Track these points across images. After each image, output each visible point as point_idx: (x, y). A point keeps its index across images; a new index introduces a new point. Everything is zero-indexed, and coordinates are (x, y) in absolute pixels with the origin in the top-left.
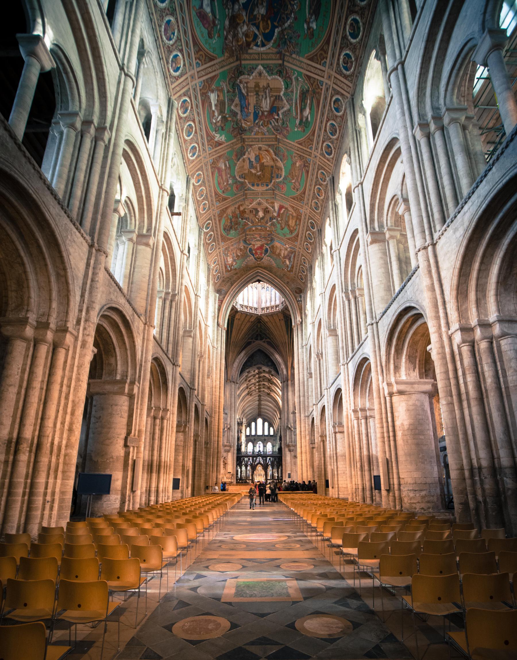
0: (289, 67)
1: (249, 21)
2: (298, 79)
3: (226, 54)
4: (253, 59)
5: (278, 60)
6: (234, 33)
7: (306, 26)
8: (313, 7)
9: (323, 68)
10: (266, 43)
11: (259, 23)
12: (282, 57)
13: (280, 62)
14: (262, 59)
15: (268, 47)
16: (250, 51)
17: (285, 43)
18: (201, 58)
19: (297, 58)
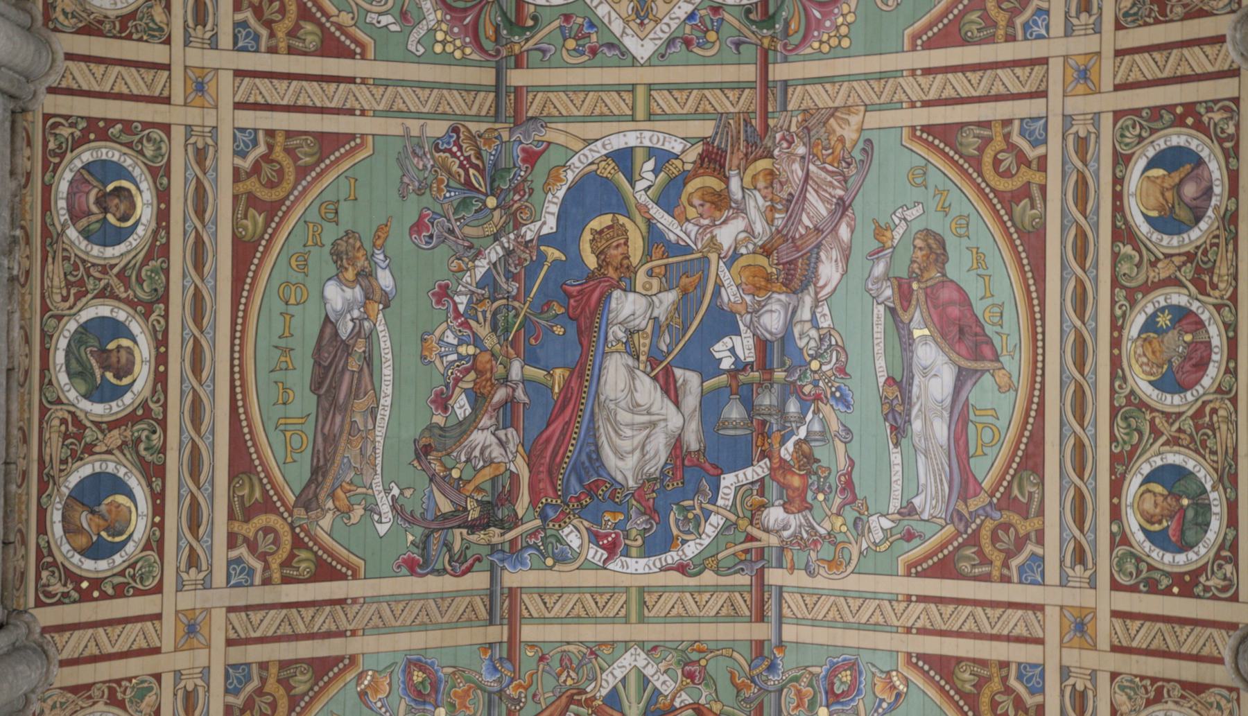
0: (464, 62)
1: (705, 259)
2: (403, 16)
3: (850, 134)
4: (686, 87)
5: (537, 89)
6: (794, 219)
7: (385, 279)
8: (354, 365)
9: (248, 119)
10: (608, 169)
11: (648, 255)
12: (509, 103)
13: (517, 78)
14: (632, 88)
15: (599, 150)
16: (706, 128)
17: (495, 174)
18: (1008, 160)
19: (414, 126)
